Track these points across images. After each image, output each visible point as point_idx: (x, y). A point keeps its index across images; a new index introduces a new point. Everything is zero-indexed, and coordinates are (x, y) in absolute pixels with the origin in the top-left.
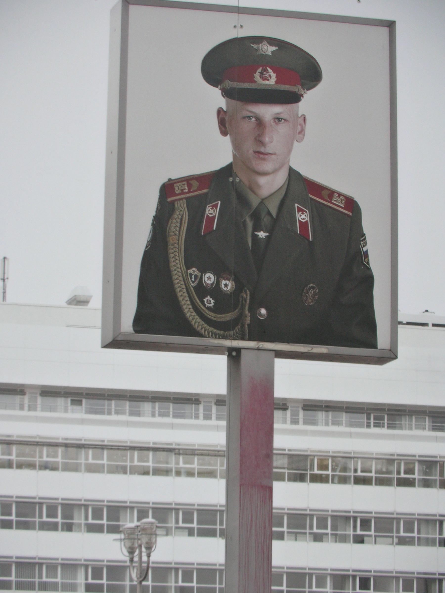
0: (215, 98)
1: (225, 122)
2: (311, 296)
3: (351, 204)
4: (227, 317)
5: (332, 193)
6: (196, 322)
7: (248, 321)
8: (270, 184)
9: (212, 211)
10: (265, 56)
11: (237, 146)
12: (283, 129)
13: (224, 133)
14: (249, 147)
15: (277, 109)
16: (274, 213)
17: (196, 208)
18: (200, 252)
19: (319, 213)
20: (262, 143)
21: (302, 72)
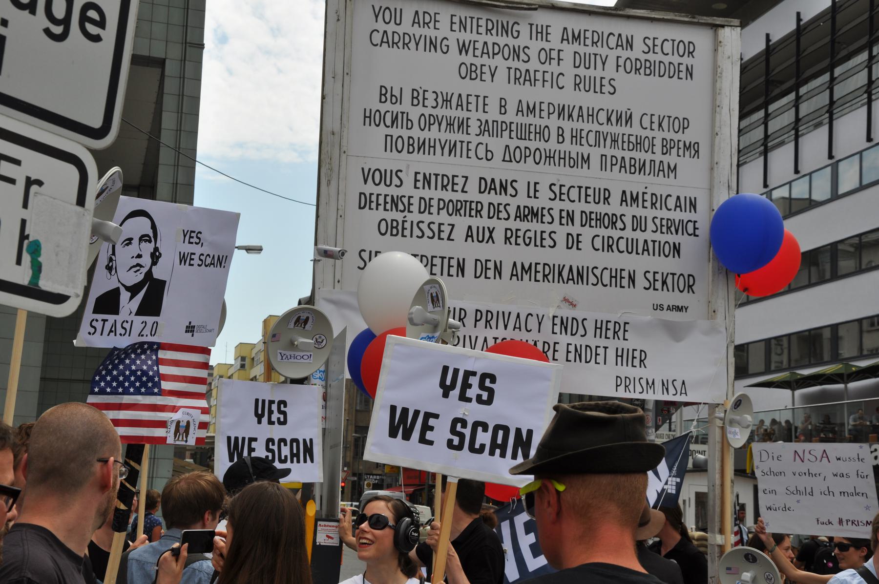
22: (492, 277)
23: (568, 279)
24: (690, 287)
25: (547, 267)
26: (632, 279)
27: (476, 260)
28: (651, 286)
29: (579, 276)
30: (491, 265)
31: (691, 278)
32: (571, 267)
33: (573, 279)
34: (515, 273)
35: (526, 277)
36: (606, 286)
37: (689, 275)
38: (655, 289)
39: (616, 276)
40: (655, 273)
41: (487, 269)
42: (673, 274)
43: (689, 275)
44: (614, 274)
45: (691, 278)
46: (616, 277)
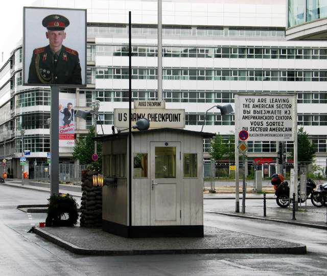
0: (45, 30)
1: (48, 35)
2: (67, 74)
3: (76, 53)
4: (49, 79)
5: (72, 50)
6: (42, 81)
7: (53, 79)
8: (58, 49)
9: (45, 56)
10: (56, 20)
11: (50, 40)
12: (61, 36)
13: (47, 38)
14: (53, 40)
15: (59, 32)
16: (58, 55)
17: (42, 57)
18: (43, 65)
19: (69, 55)
20: (56, 40)
21: (65, 22)
29: (274, 135)
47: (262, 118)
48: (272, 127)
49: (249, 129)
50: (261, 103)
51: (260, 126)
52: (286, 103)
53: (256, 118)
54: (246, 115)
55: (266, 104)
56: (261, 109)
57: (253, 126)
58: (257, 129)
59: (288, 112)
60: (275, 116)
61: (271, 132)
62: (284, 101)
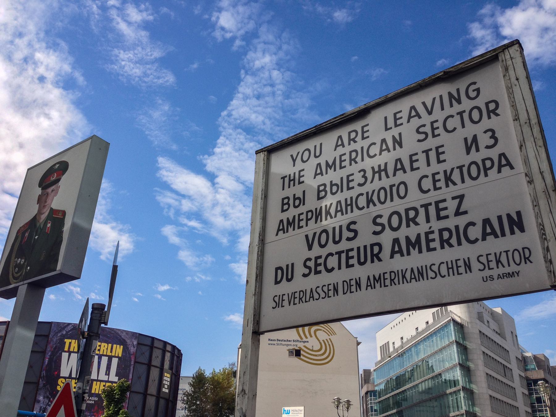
22: (355, 290)
23: (411, 279)
24: (525, 258)
25: (393, 274)
26: (468, 266)
27: (343, 282)
28: (486, 266)
29: (420, 274)
30: (353, 282)
31: (527, 251)
32: (412, 269)
33: (415, 278)
34: (369, 284)
35: (377, 285)
36: (445, 276)
37: (523, 249)
38: (489, 269)
39: (453, 268)
40: (487, 255)
41: (351, 286)
42: (507, 252)
43: (523, 249)
44: (450, 266)
45: (527, 251)
46: (452, 268)
47: (351, 204)
48: (402, 234)
49: (300, 270)
50: (347, 149)
51: (344, 245)
52: (467, 105)
53: (328, 213)
54: (292, 212)
55: (365, 144)
56: (344, 173)
57: (317, 251)
58: (332, 262)
59: (484, 140)
60: (411, 178)
61: (400, 263)
62: (455, 99)
